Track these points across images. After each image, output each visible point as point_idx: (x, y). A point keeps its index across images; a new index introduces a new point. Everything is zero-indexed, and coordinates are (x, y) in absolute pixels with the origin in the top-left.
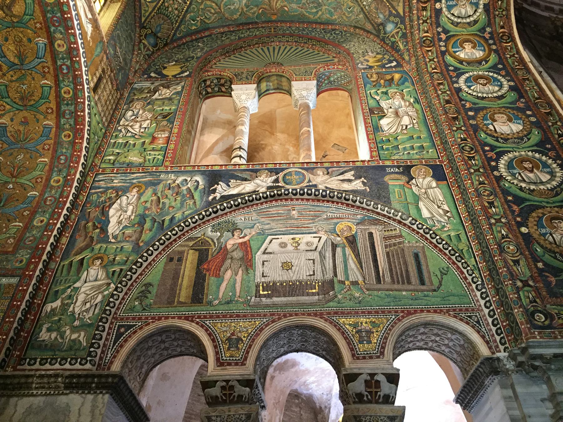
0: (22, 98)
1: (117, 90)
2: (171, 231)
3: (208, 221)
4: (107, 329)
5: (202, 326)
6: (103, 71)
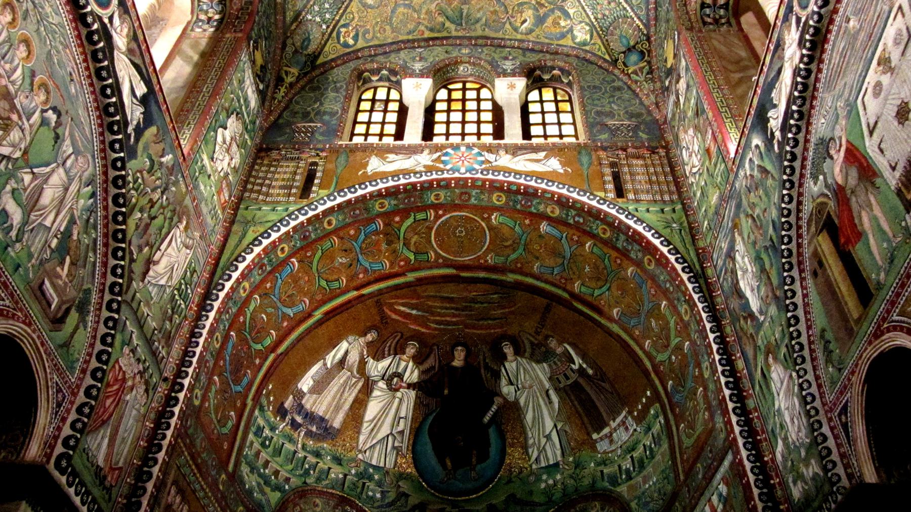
0: (598, 279)
1: (653, 151)
2: (783, 244)
3: (802, 176)
4: (828, 433)
5: (895, 329)
6: (613, 165)
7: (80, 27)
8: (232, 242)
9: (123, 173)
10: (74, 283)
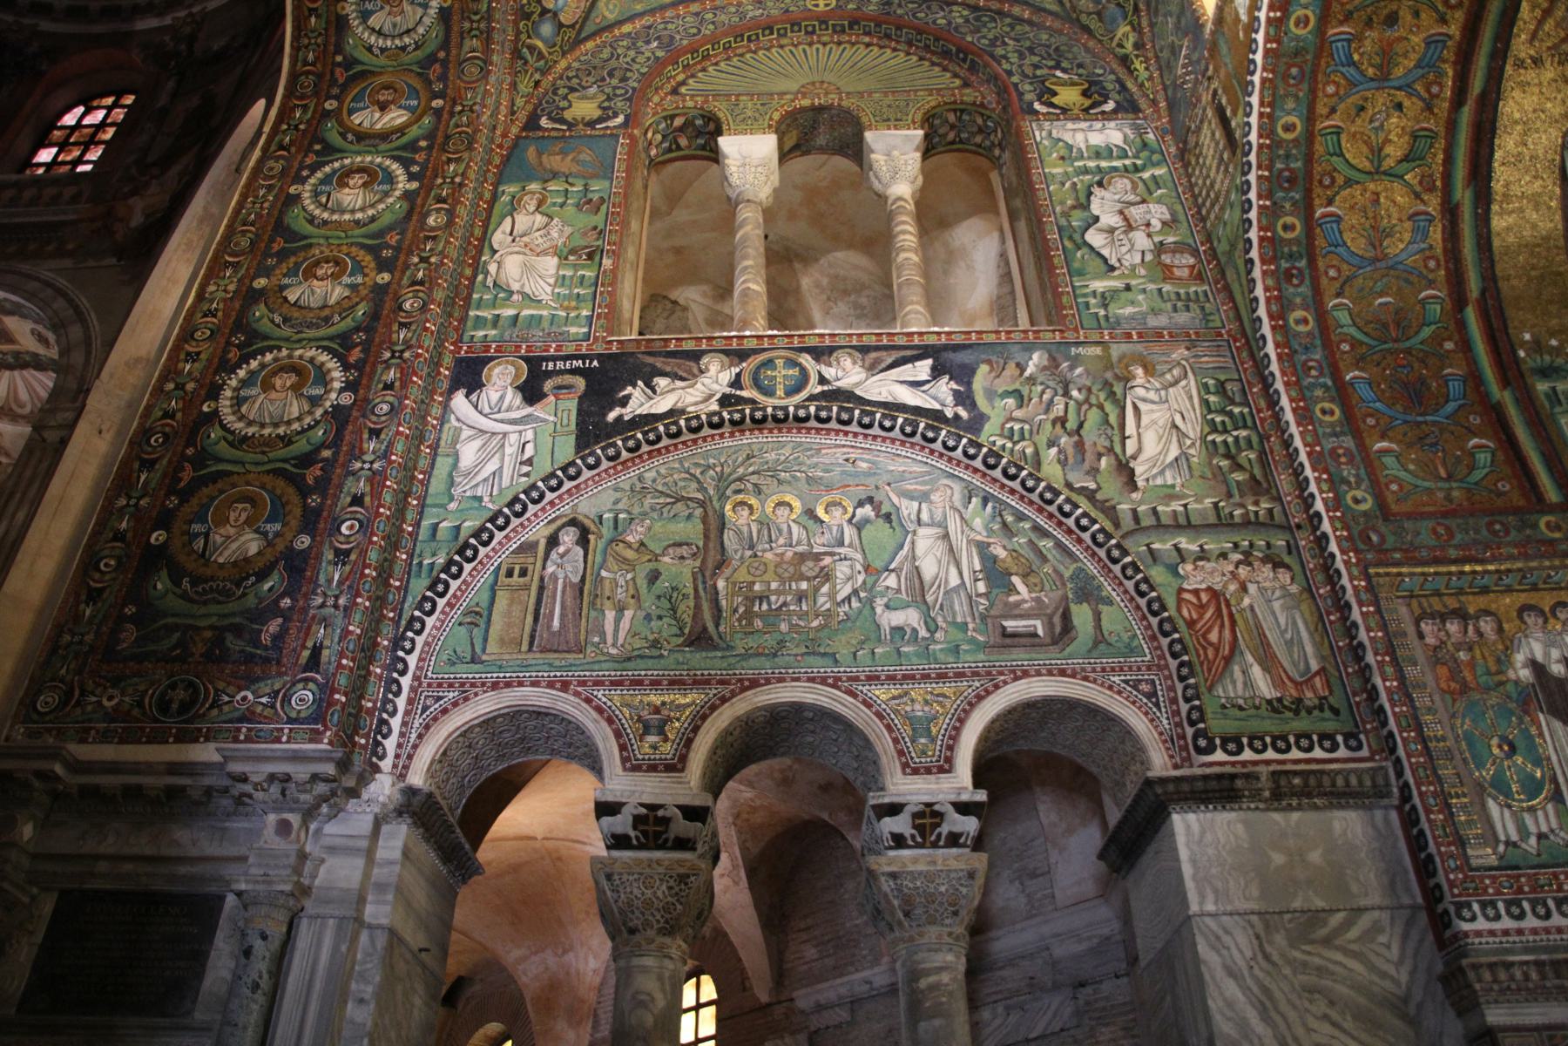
7: (808, 425)
8: (1238, 297)
9: (985, 450)
10: (1047, 587)
